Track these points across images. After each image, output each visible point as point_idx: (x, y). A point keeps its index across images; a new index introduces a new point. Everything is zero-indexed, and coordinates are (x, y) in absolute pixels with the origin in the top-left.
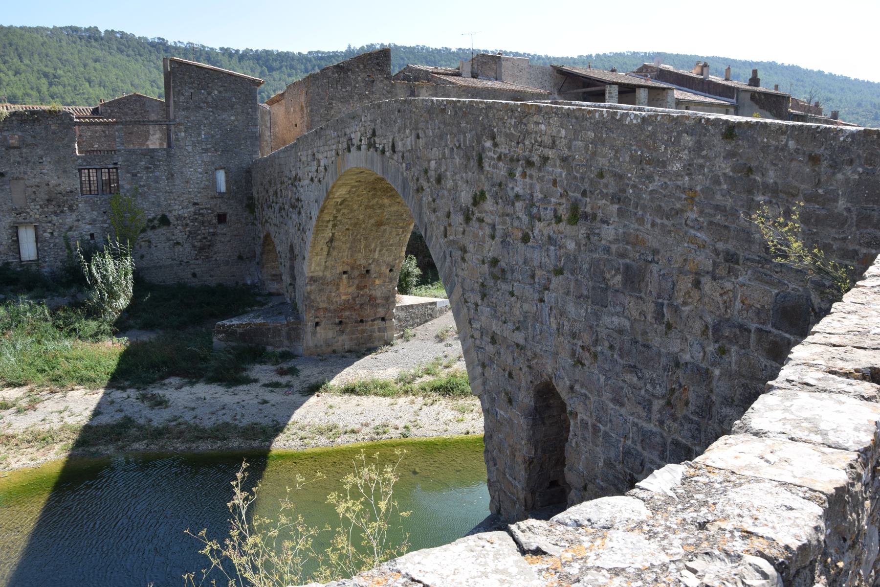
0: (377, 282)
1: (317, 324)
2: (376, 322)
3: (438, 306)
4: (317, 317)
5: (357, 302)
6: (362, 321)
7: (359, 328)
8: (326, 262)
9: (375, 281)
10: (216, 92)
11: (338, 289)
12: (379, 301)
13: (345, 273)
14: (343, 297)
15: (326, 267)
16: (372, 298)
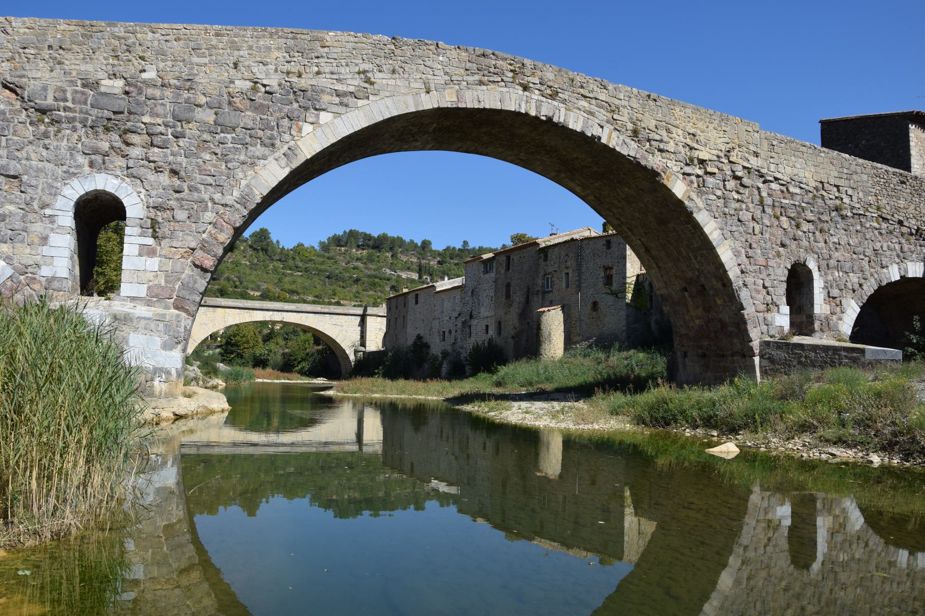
0: (719, 302)
1: (685, 355)
2: (735, 358)
3: (868, 356)
4: (683, 346)
5: (711, 329)
6: (723, 356)
7: (722, 364)
8: (662, 276)
9: (716, 301)
10: (864, 142)
11: (688, 311)
12: (731, 329)
13: (685, 289)
14: (697, 322)
15: (665, 283)
16: (724, 325)
